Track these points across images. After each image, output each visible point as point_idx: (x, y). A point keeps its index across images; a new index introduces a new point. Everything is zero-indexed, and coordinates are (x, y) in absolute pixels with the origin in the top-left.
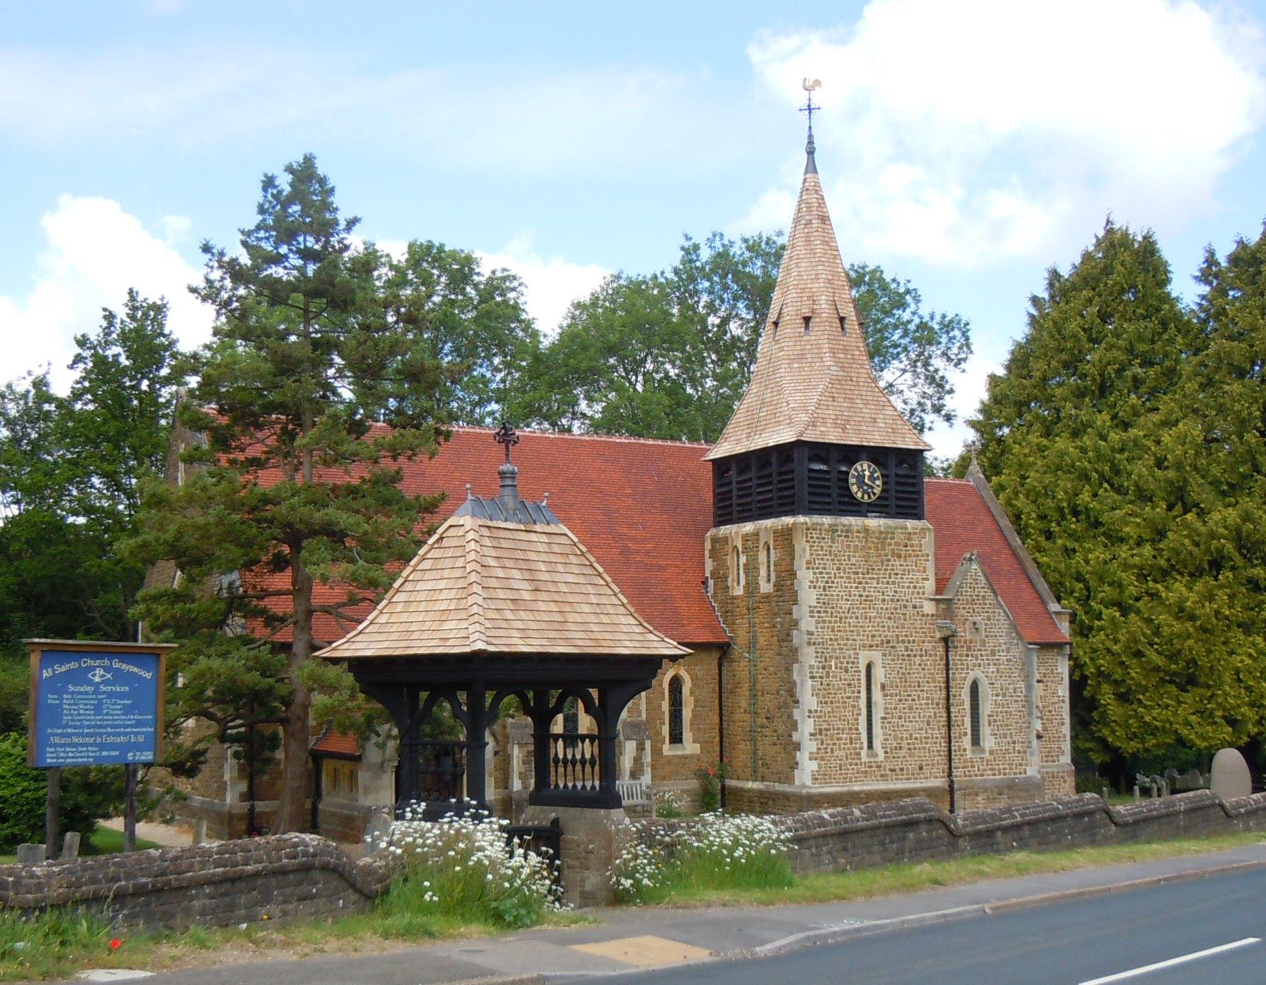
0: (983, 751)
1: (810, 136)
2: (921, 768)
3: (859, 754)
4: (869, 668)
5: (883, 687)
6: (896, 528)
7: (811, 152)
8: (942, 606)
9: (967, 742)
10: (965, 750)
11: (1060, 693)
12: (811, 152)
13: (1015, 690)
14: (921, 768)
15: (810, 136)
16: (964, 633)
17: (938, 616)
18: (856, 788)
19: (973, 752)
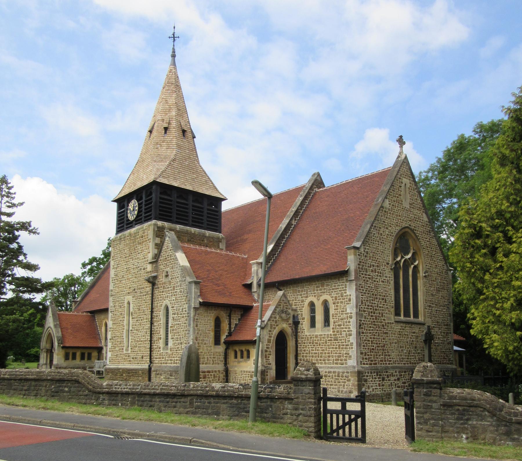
0: (167, 349)
1: (174, 49)
2: (142, 358)
3: (123, 349)
4: (129, 303)
5: (132, 314)
6: (140, 229)
7: (174, 56)
8: (154, 266)
9: (161, 343)
10: (160, 348)
11: (348, 311)
12: (174, 56)
13: (182, 309)
14: (142, 358)
15: (174, 49)
16: (162, 279)
17: (153, 272)
18: (120, 367)
19: (163, 349)
